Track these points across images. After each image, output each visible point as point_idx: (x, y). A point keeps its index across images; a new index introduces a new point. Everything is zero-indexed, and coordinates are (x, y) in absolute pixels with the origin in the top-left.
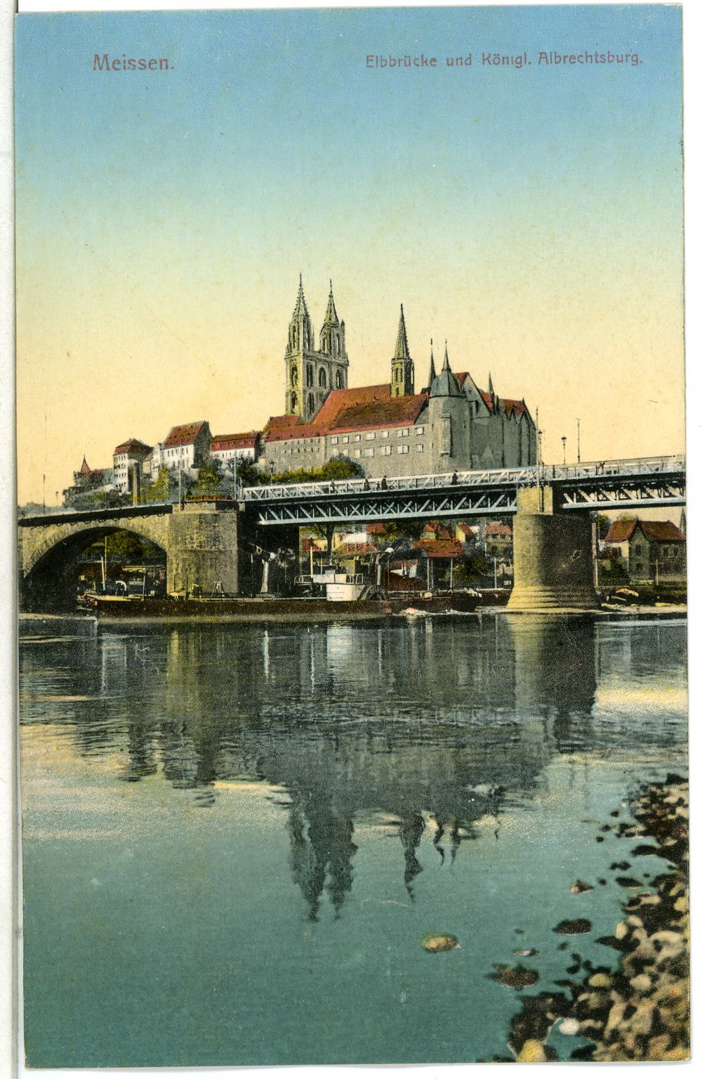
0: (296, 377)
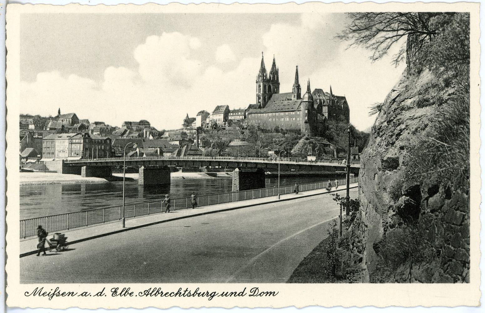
0: (260, 89)
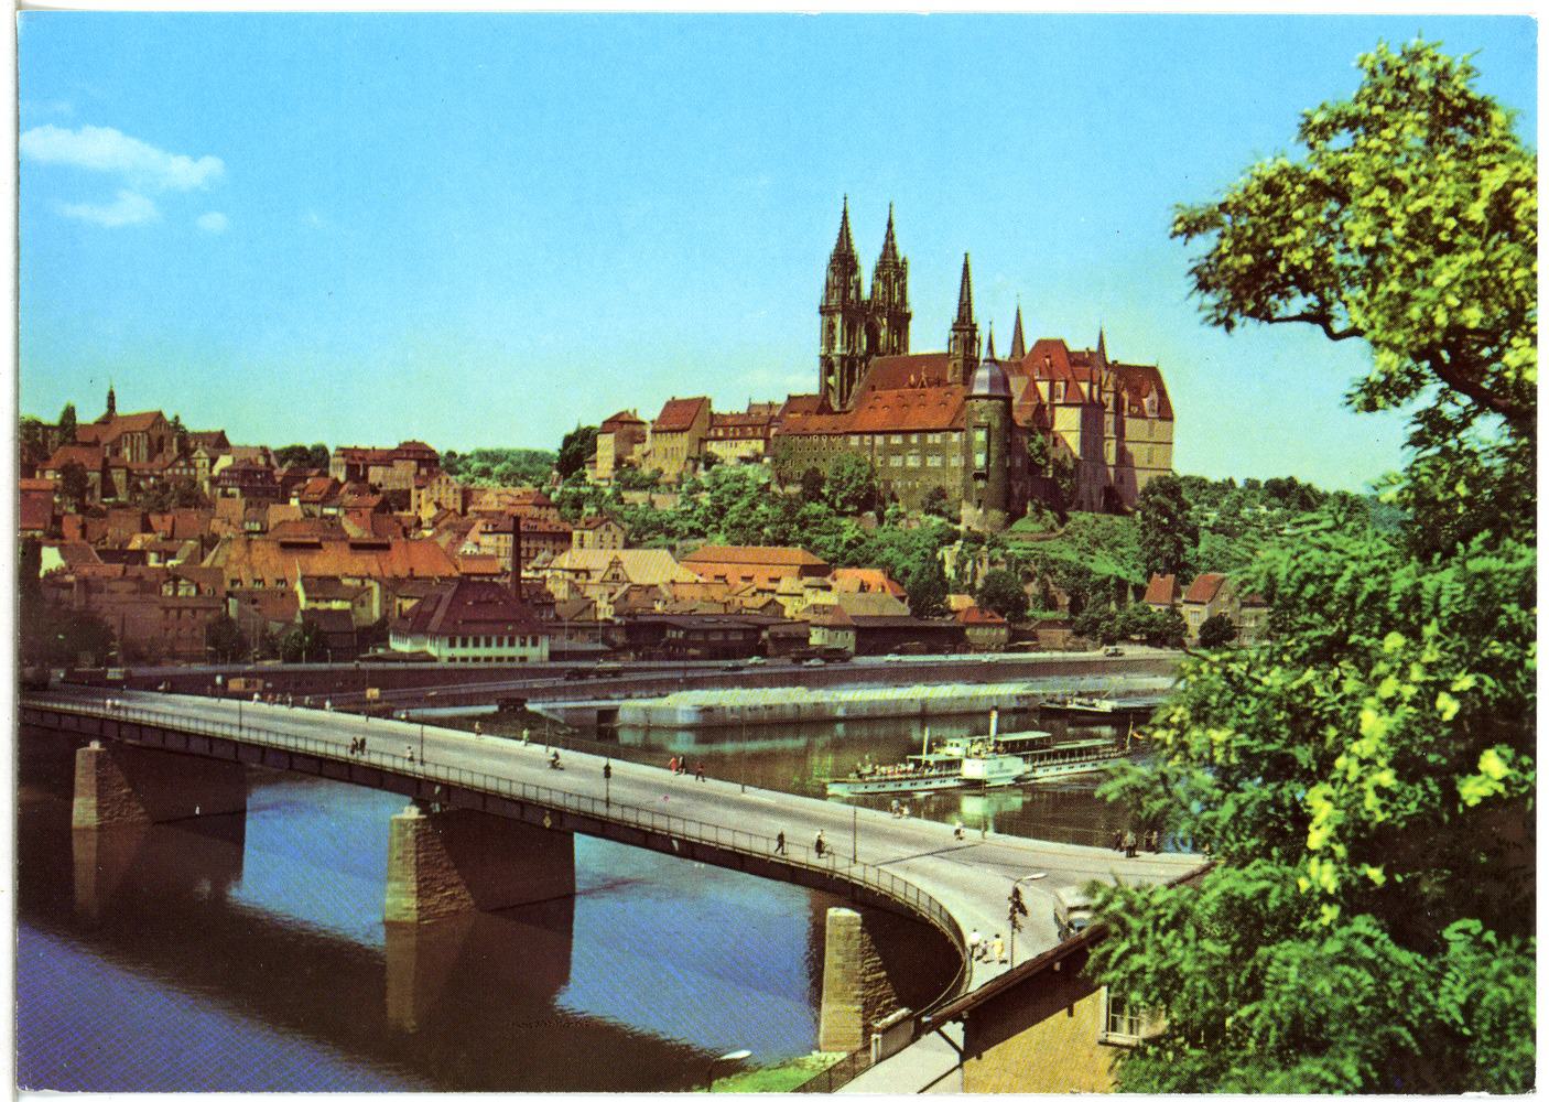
0: (834, 338)
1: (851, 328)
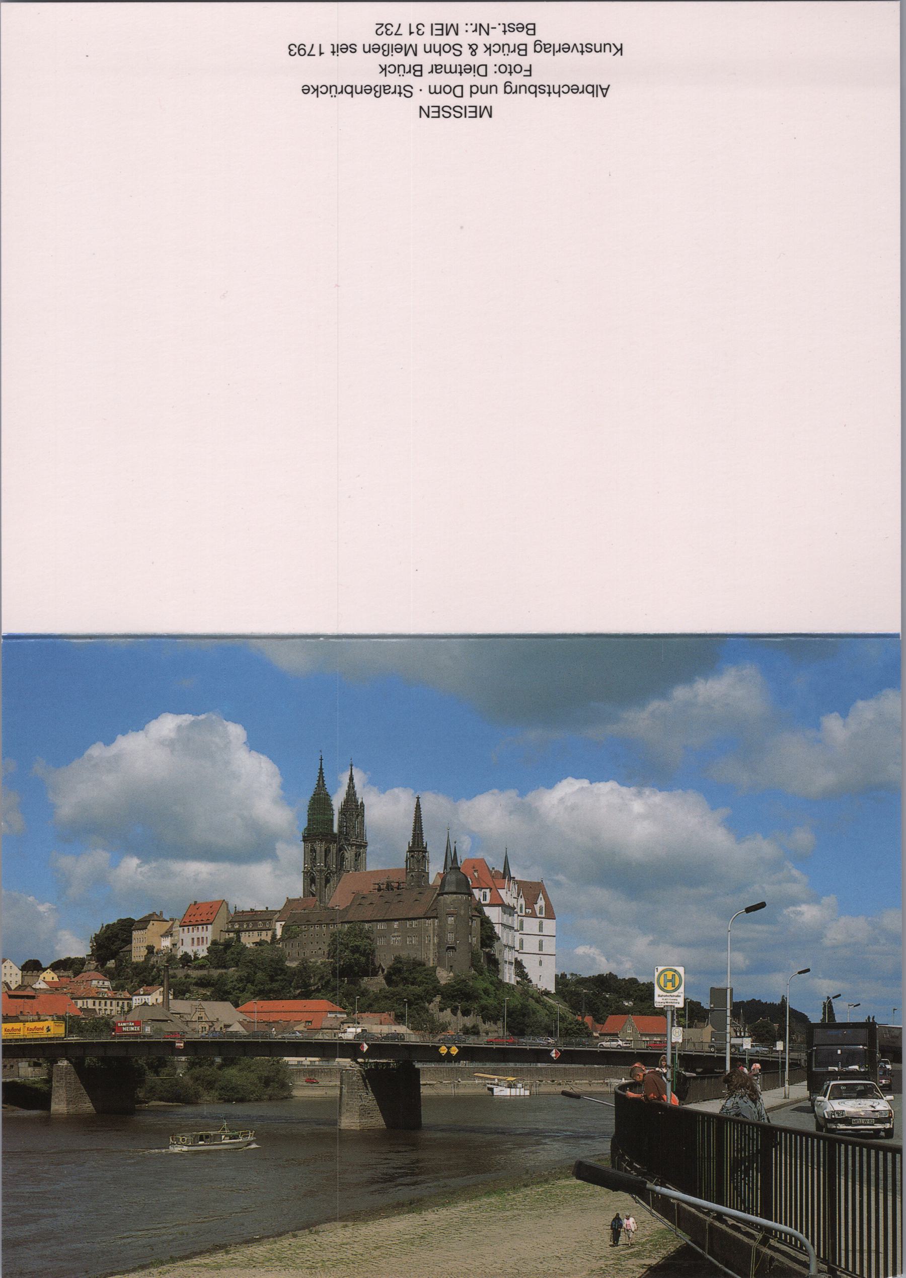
1: (327, 852)
